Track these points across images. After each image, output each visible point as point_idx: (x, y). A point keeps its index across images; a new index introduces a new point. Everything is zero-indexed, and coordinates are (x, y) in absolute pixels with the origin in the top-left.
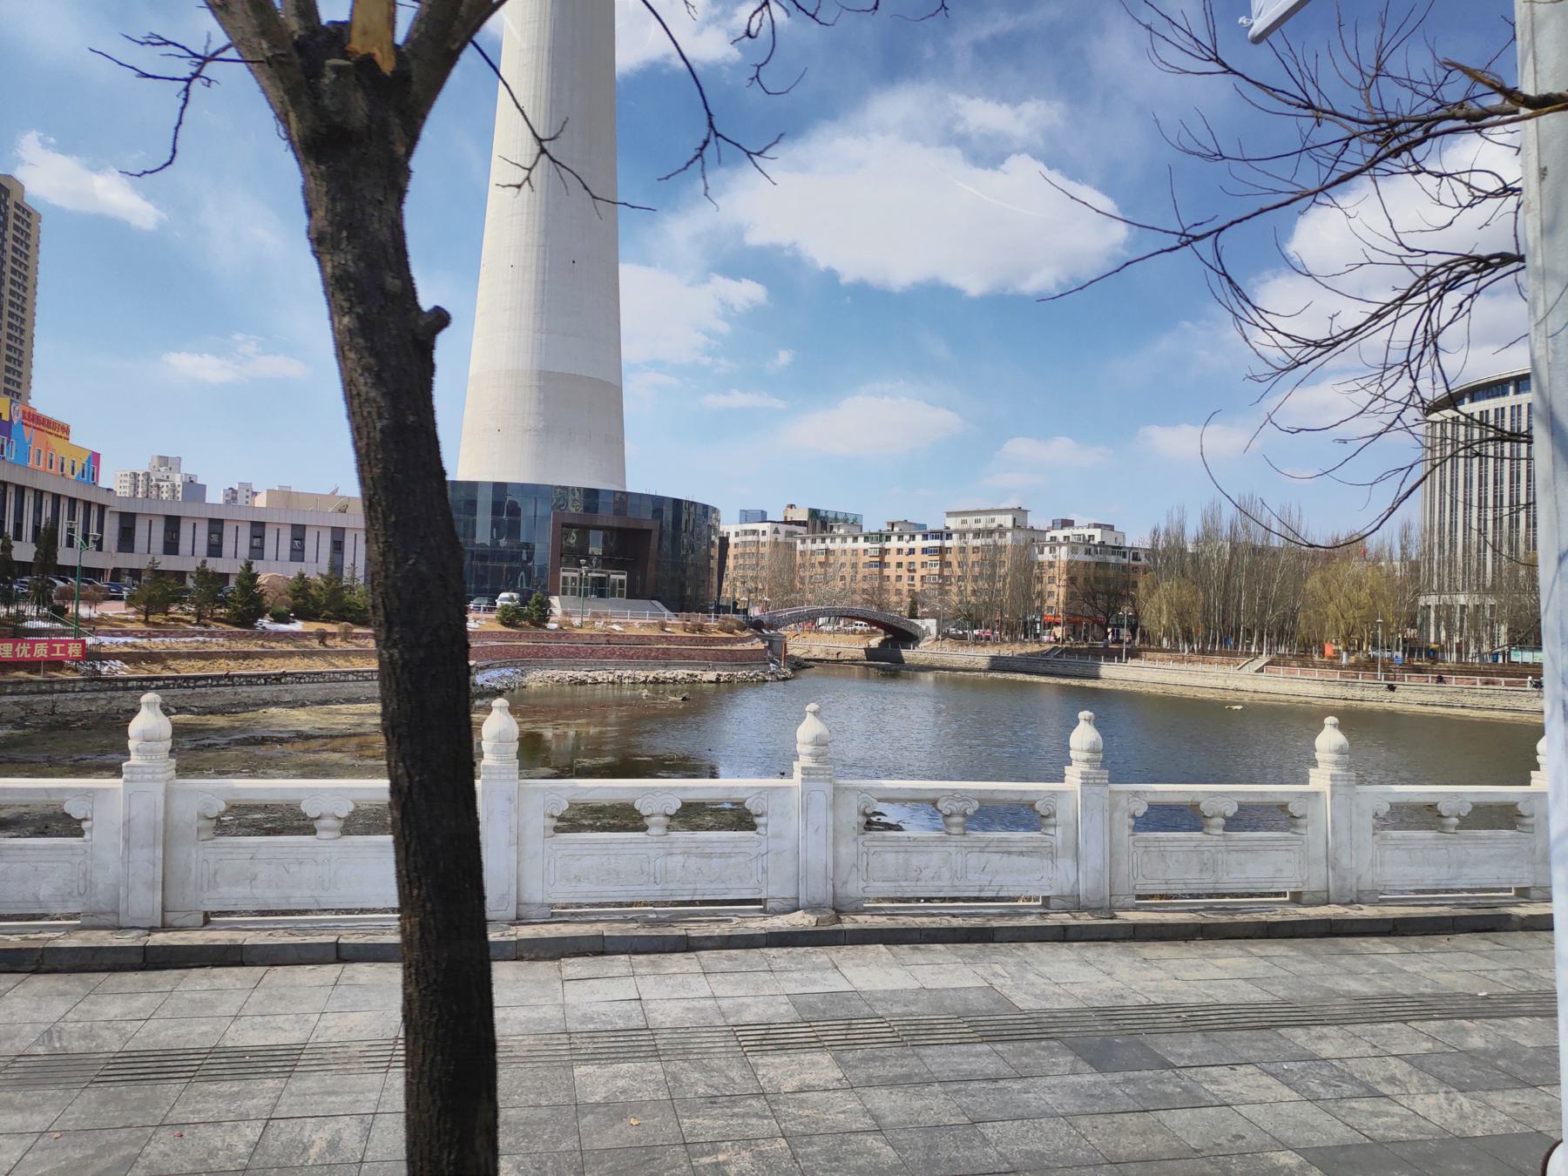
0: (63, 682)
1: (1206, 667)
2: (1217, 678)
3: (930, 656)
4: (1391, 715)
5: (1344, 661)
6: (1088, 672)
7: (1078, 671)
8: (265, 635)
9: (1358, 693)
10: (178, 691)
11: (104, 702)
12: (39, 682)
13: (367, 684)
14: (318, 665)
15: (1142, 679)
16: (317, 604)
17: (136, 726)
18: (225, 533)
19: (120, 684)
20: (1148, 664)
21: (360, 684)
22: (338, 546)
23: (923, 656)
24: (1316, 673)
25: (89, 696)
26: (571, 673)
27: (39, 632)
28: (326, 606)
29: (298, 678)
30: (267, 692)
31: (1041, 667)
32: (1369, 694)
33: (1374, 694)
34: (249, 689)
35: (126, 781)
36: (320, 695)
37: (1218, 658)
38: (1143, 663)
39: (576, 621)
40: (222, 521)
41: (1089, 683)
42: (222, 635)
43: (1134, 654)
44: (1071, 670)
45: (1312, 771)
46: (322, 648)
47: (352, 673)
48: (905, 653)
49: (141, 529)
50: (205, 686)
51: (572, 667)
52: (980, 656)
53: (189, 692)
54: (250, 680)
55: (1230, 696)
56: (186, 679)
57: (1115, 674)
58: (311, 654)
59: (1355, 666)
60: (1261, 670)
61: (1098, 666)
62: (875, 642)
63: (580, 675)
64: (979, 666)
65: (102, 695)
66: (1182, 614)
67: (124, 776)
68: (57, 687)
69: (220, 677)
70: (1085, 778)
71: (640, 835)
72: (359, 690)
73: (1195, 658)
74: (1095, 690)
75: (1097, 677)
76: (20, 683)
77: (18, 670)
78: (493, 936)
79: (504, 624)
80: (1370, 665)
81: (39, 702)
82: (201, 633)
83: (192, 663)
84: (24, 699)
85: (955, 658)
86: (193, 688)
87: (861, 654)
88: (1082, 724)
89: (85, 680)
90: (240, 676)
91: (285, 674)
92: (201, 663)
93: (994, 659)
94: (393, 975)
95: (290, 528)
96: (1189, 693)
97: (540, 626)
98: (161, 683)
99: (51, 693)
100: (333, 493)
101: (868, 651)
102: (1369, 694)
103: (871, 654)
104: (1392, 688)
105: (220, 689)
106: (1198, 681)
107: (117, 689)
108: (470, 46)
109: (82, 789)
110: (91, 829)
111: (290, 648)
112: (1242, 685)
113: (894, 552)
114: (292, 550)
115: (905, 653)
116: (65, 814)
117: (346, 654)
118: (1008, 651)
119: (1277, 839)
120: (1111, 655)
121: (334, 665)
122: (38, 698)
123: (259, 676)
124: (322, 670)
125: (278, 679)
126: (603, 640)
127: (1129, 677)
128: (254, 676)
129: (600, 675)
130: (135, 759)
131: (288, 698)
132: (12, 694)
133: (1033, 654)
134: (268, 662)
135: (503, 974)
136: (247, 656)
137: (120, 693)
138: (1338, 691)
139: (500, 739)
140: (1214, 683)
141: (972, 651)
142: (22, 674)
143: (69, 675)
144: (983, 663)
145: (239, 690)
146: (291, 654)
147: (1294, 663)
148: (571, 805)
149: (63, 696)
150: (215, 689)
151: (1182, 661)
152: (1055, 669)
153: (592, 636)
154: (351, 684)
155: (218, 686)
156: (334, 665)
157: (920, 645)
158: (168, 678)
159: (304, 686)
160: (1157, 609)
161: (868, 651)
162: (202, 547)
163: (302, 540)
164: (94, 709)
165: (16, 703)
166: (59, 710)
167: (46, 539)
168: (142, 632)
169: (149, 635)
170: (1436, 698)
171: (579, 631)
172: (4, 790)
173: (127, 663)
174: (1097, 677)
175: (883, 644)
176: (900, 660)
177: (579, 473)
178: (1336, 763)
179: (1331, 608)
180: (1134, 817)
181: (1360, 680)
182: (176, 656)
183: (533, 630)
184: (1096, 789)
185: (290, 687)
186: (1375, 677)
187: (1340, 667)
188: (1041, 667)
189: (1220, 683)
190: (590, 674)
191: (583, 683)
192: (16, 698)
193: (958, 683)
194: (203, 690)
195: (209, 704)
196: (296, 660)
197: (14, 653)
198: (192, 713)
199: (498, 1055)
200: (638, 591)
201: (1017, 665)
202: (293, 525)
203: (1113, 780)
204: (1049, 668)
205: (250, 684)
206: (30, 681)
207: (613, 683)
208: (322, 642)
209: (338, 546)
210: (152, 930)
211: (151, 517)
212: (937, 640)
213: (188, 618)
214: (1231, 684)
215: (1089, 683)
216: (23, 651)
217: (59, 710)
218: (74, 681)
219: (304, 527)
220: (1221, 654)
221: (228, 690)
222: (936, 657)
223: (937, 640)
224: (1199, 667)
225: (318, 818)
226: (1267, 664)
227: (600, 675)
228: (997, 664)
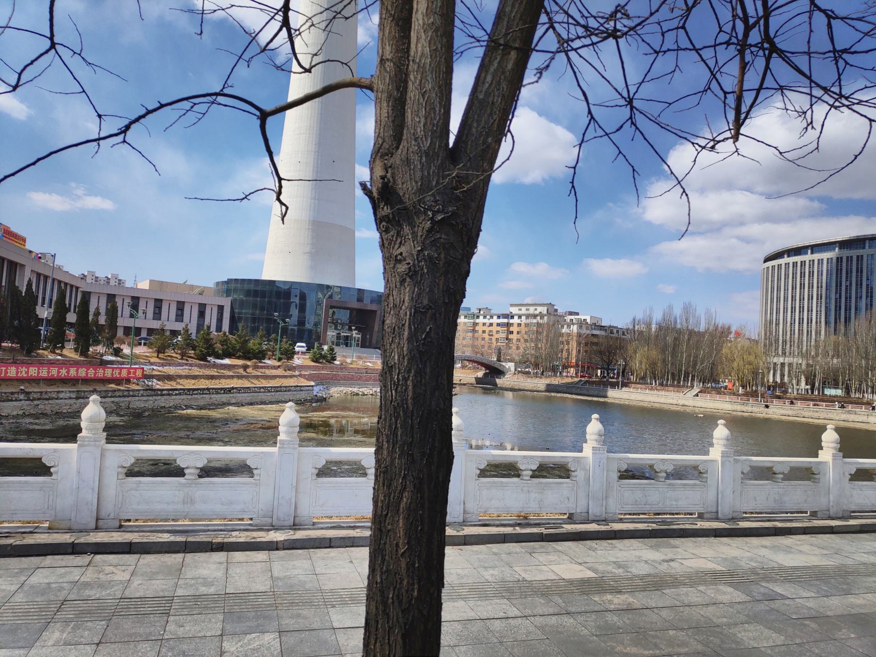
0: (133, 390)
1: (667, 393)
2: (673, 399)
3: (512, 383)
4: (767, 421)
5: (740, 392)
6: (601, 393)
7: (596, 393)
8: (215, 366)
9: (750, 409)
10: (184, 397)
11: (152, 402)
12: (123, 390)
13: (269, 394)
14: (246, 384)
15: (631, 398)
16: (234, 348)
17: (86, 414)
18: (163, 307)
19: (159, 393)
20: (634, 390)
21: (266, 394)
22: (202, 314)
23: (508, 383)
24: (727, 398)
25: (145, 398)
26: (351, 389)
27: (111, 362)
28: (239, 350)
29: (239, 390)
30: (224, 398)
31: (574, 390)
32: (755, 409)
33: (758, 410)
34: (216, 396)
35: (80, 446)
36: (248, 400)
37: (671, 388)
38: (631, 390)
39: (349, 360)
40: (139, 298)
41: (602, 400)
42: (196, 366)
43: (625, 385)
44: (592, 392)
45: (820, 452)
46: (245, 374)
47: (263, 388)
48: (498, 381)
49: (142, 306)
50: (197, 394)
51: (350, 386)
52: (541, 383)
53: (189, 397)
54: (217, 391)
55: (697, 410)
56: (189, 390)
57: (615, 395)
58: (240, 377)
59: (746, 394)
60: (697, 395)
61: (606, 391)
62: (480, 374)
63: (355, 390)
64: (540, 389)
65: (151, 398)
66: (653, 365)
67: (78, 442)
68: (131, 393)
69: (204, 389)
70: (724, 455)
71: (515, 480)
72: (265, 397)
73: (659, 388)
74: (605, 403)
75: (606, 397)
76: (115, 391)
77: (110, 383)
78: (449, 531)
79: (313, 361)
80: (754, 394)
81: (123, 402)
82: (186, 364)
83: (189, 381)
84: (116, 400)
85: (526, 384)
86: (192, 395)
87: (473, 381)
88: (720, 426)
89: (144, 390)
90: (213, 389)
91: (233, 388)
92: (193, 381)
93: (548, 385)
94: (363, 554)
95: (176, 303)
96: (666, 407)
97: (331, 363)
98: (177, 392)
99: (128, 397)
100: (185, 283)
101: (476, 379)
102: (755, 409)
103: (479, 381)
104: (767, 407)
105: (204, 396)
106: (662, 400)
107: (157, 395)
108: (740, 136)
109: (188, 451)
110: (57, 473)
111: (231, 374)
112: (686, 403)
113: (515, 325)
114: (177, 315)
115: (498, 381)
116: (247, 465)
117: (257, 377)
118: (556, 381)
119: (766, 485)
120: (614, 385)
121: (252, 383)
122: (122, 399)
123: (221, 389)
124: (249, 386)
125: (229, 391)
126: (364, 371)
127: (624, 397)
128: (219, 389)
129: (366, 391)
130: (84, 433)
131: (233, 401)
132: (111, 397)
133: (569, 383)
134: (223, 381)
135: (450, 552)
136: (212, 377)
137: (159, 397)
138: (739, 408)
139: (290, 425)
140: (671, 401)
141: (536, 381)
142: (113, 386)
143: (134, 387)
144: (542, 387)
145: (212, 396)
146: (232, 377)
147: (714, 392)
148: (327, 462)
149: (133, 399)
150: (202, 396)
151: (652, 389)
152: (582, 392)
153: (358, 369)
154: (262, 394)
155: (203, 394)
156: (252, 383)
157: (506, 377)
158: (181, 389)
159: (241, 395)
160: (638, 362)
161: (476, 379)
162: (150, 314)
163: (160, 308)
164: (147, 406)
165: (113, 402)
166: (131, 406)
167: (112, 313)
168: (159, 363)
169: (163, 365)
170: (790, 412)
171: (351, 366)
172: (2, 449)
173: (159, 381)
174: (606, 397)
175: (485, 374)
176: (495, 384)
177: (333, 278)
178: (835, 448)
179: (735, 365)
180: (743, 473)
181: (863, 410)
182: (180, 377)
183: (329, 365)
184: (838, 461)
185: (235, 395)
186: (757, 400)
187: (739, 395)
188: (574, 390)
189: (675, 402)
190: (360, 390)
191: (357, 394)
192: (113, 399)
193: (534, 398)
194: (196, 396)
195: (199, 404)
196: (235, 380)
197: (112, 374)
198: (193, 409)
199: (442, 594)
200: (367, 344)
201: (560, 389)
202: (199, 304)
203: (844, 457)
204: (579, 391)
205: (217, 393)
206: (119, 390)
207: (372, 395)
208: (245, 370)
209: (202, 314)
210: (87, 531)
211: (99, 295)
212: (515, 374)
213: (177, 356)
214: (681, 402)
215: (602, 400)
216: (100, 373)
217: (131, 406)
218: (139, 390)
219: (184, 302)
220: (672, 386)
221: (207, 396)
222: (516, 383)
223: (515, 374)
224: (663, 393)
225: (186, 468)
226: (699, 392)
227: (366, 391)
228: (550, 388)
